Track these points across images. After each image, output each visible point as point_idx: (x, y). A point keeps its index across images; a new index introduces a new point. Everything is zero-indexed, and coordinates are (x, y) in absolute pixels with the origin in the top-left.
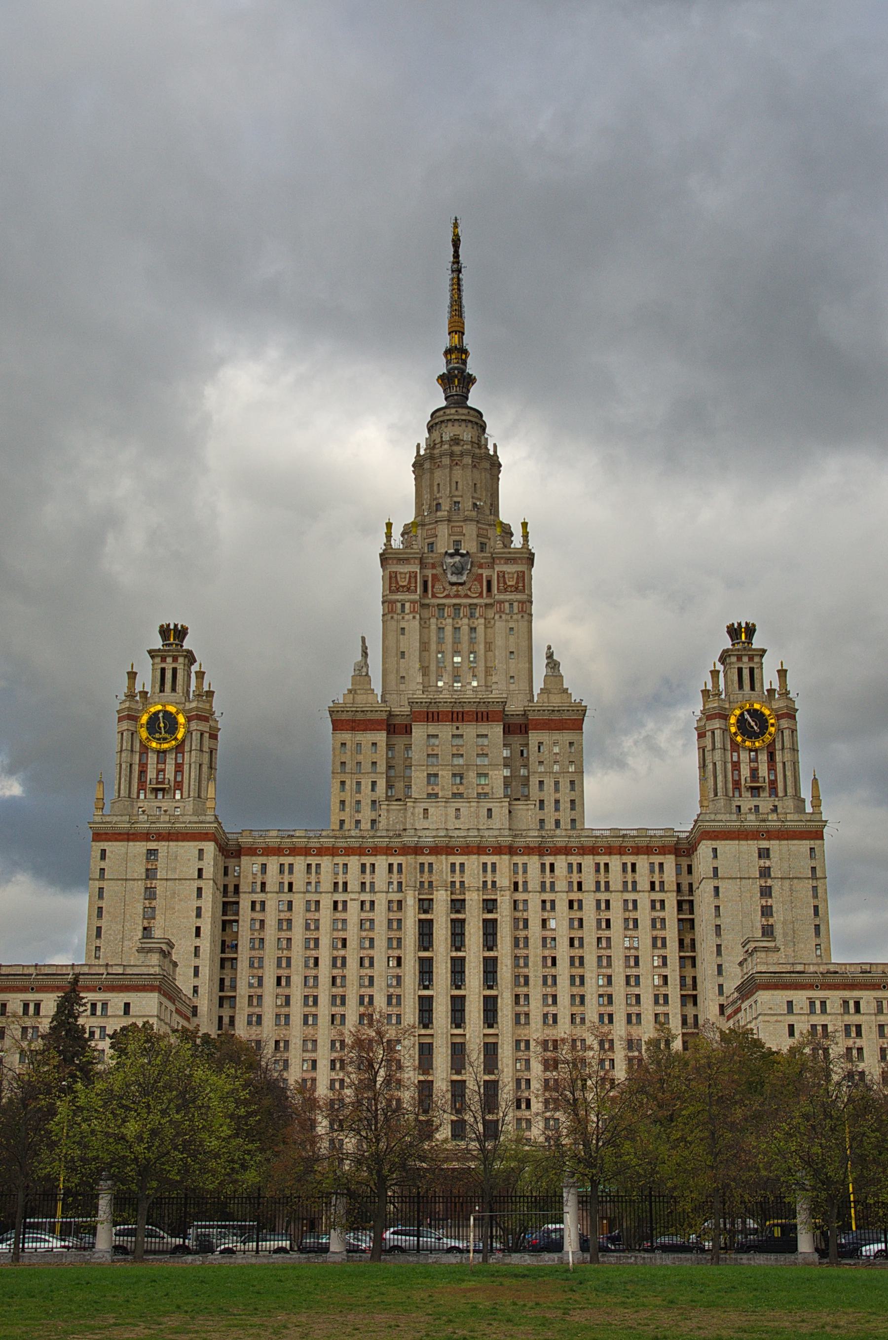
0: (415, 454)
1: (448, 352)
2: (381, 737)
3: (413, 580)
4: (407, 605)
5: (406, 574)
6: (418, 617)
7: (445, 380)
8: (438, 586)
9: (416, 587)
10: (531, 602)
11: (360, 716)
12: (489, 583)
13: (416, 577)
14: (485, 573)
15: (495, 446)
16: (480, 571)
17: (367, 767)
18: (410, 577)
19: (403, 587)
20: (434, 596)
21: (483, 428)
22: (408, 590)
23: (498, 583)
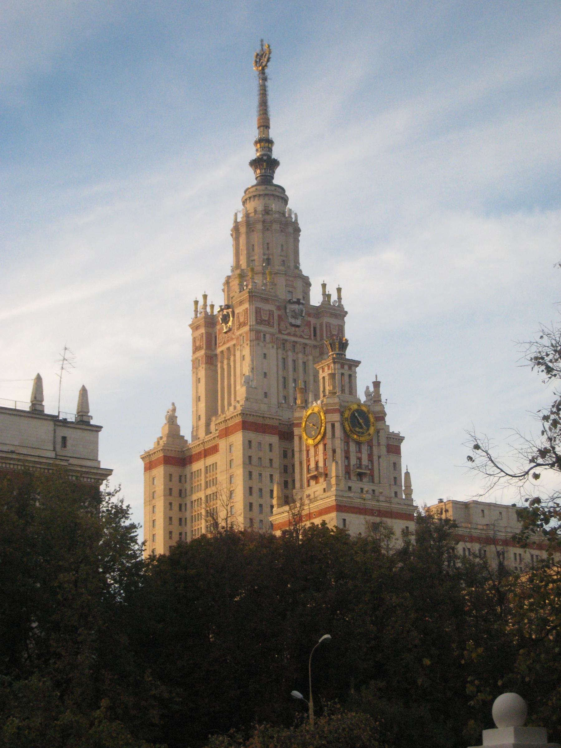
2: (274, 439)
3: (271, 317)
4: (268, 336)
5: (266, 311)
6: (275, 346)
8: (282, 325)
11: (261, 421)
12: (315, 329)
14: (313, 321)
17: (266, 463)
18: (270, 314)
19: (265, 321)
22: (269, 324)
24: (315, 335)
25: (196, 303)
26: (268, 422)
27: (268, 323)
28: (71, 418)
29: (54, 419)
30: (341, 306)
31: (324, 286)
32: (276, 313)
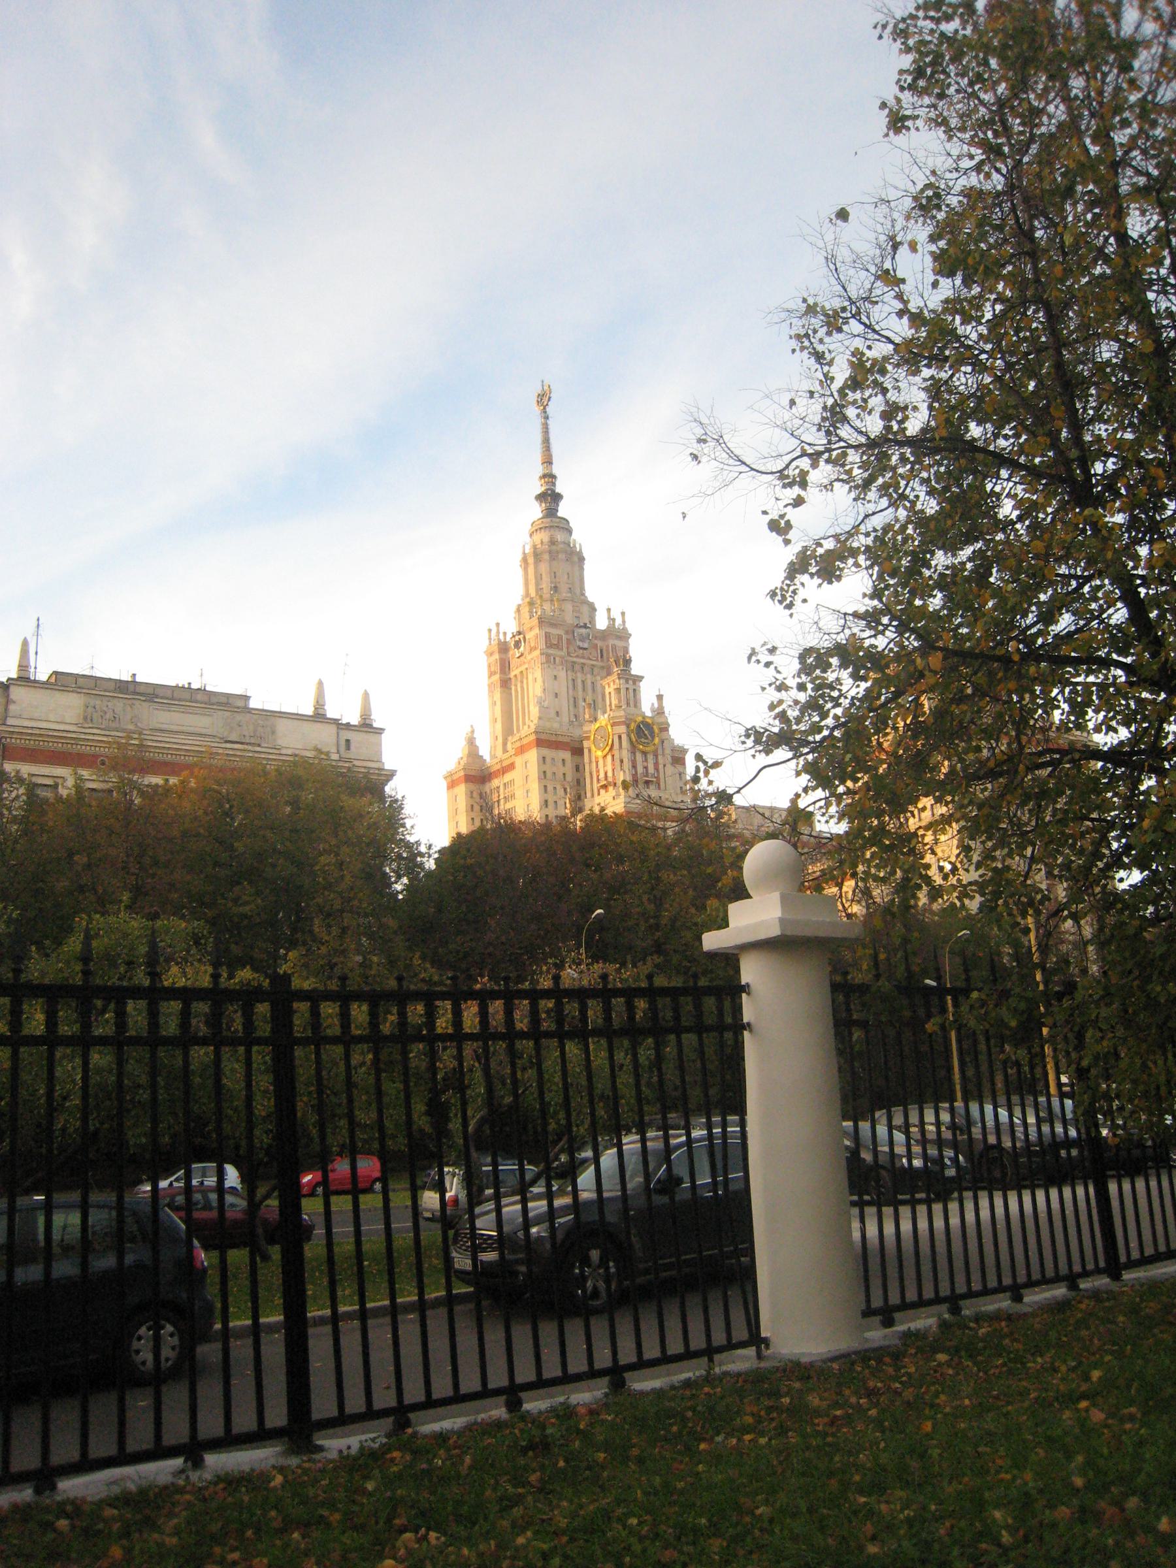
2: (567, 755)
7: (541, 497)
11: (553, 738)
14: (599, 643)
24: (602, 656)
25: (490, 631)
26: (560, 739)
27: (557, 646)
28: (355, 720)
29: (336, 722)
30: (625, 629)
31: (609, 610)
32: (564, 637)
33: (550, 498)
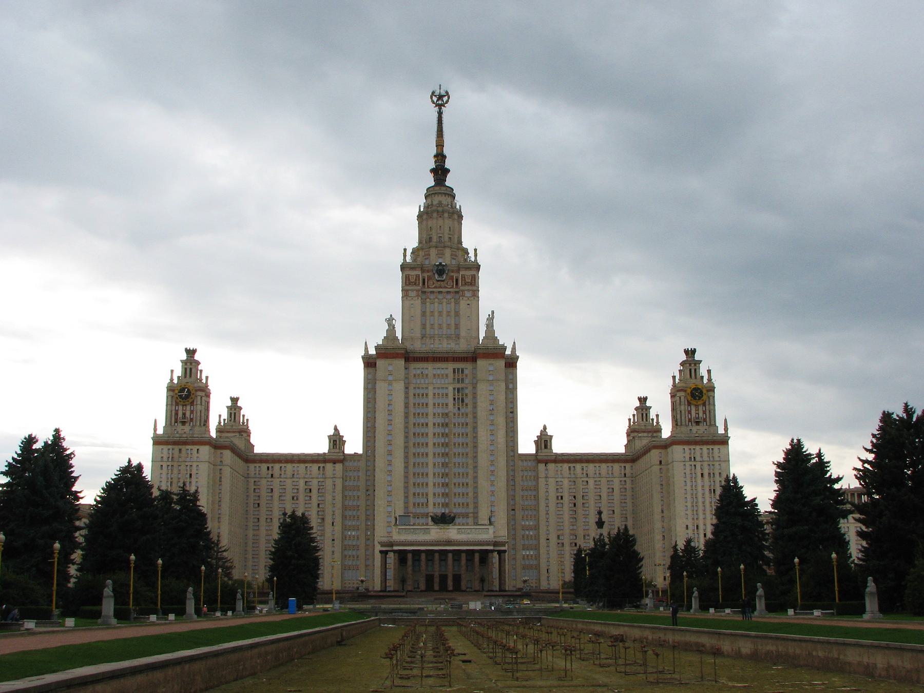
0: (418, 211)
1: (435, 156)
3: (417, 279)
5: (414, 276)
9: (419, 283)
10: (479, 291)
12: (457, 280)
13: (419, 276)
14: (455, 275)
15: (460, 207)
16: (452, 274)
20: (428, 287)
21: (453, 197)
23: (462, 281)
24: (457, 284)
33: (440, 172)
